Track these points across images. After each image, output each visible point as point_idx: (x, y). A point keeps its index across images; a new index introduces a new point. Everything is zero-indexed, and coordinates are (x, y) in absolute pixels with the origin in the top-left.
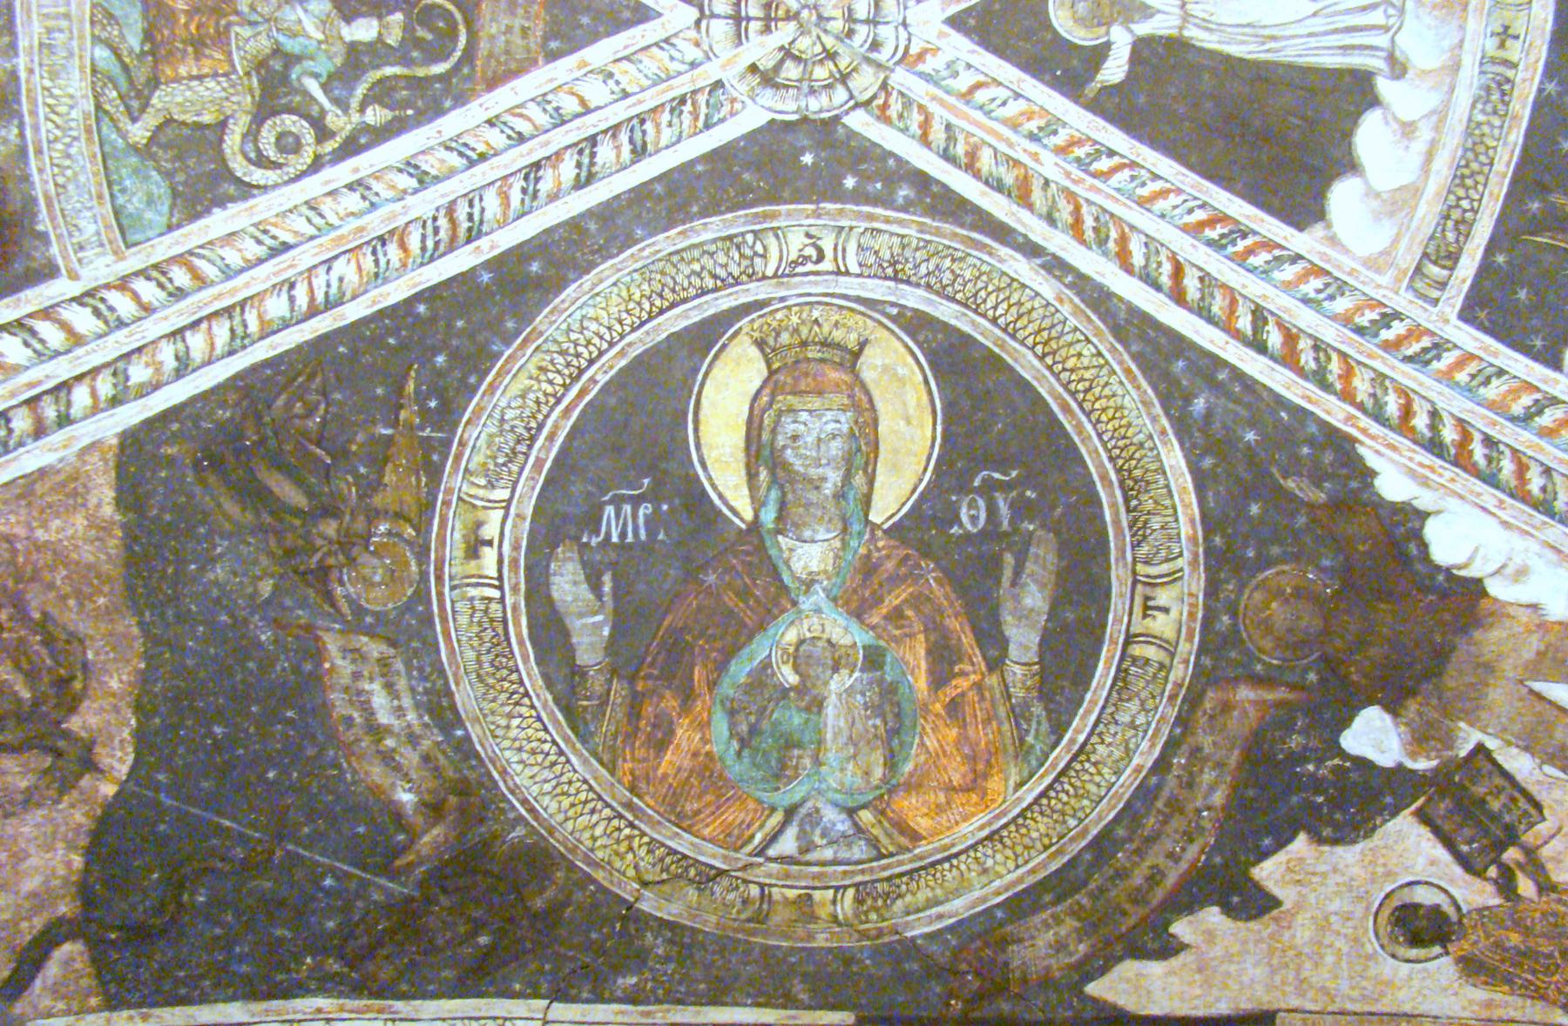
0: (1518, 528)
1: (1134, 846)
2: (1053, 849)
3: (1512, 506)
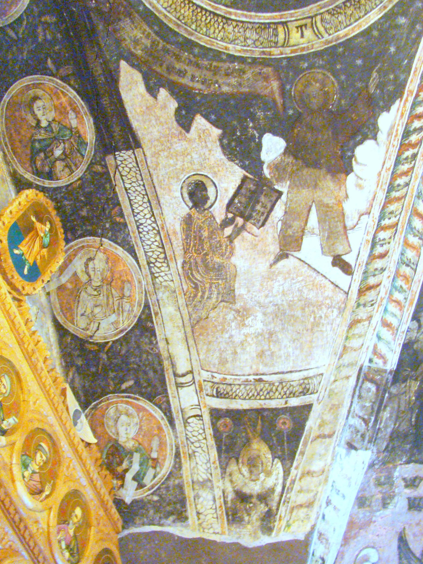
0: (379, 180)
1: (192, 59)
2: (179, 22)
3: (388, 175)
